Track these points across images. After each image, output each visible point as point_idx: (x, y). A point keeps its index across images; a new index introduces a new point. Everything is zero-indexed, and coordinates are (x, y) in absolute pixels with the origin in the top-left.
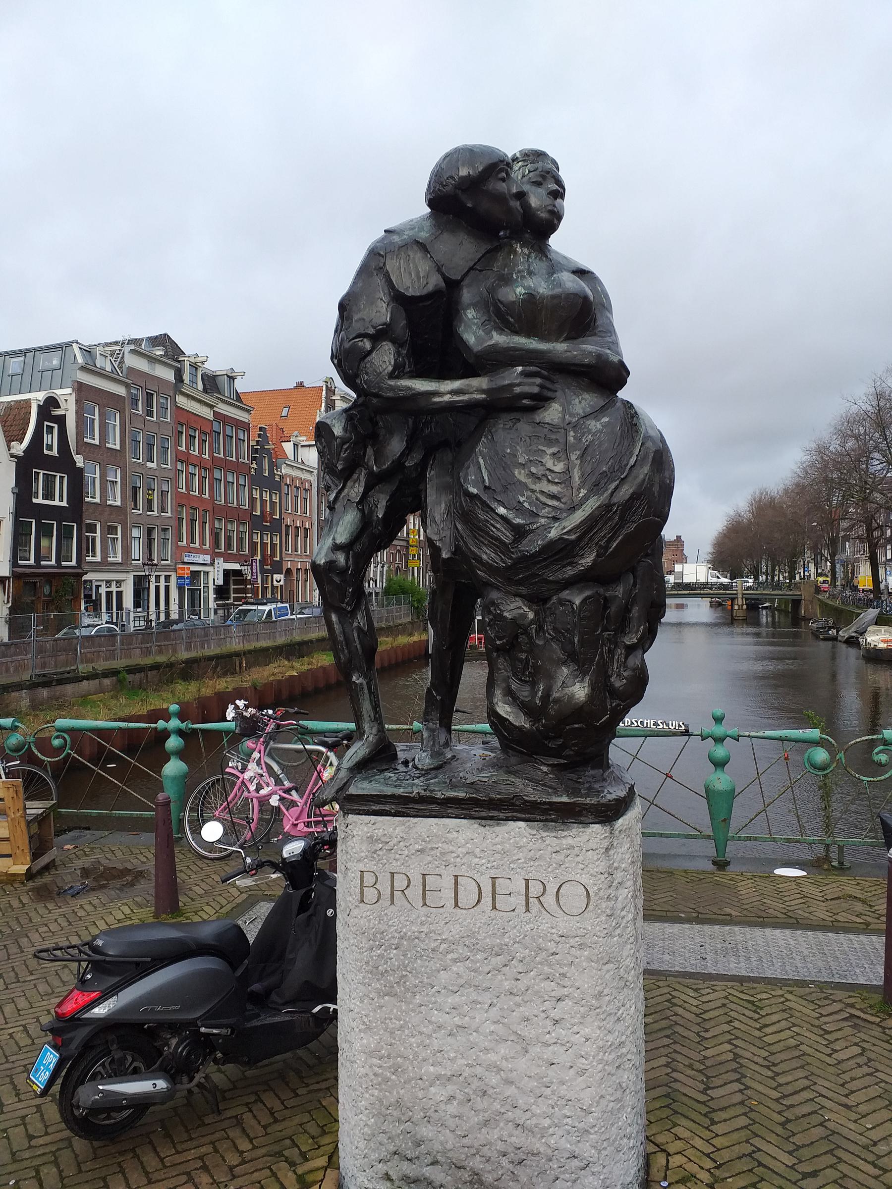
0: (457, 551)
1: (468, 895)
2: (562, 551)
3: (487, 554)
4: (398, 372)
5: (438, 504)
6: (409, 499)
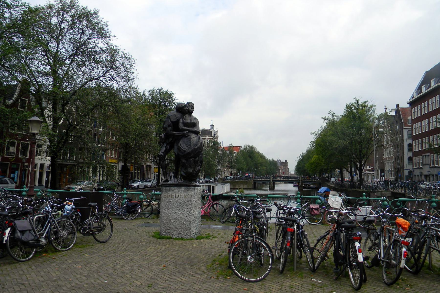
0: (178, 153)
1: (177, 196)
2: (189, 154)
3: (181, 154)
4: (171, 131)
5: (176, 147)
6: (172, 147)
